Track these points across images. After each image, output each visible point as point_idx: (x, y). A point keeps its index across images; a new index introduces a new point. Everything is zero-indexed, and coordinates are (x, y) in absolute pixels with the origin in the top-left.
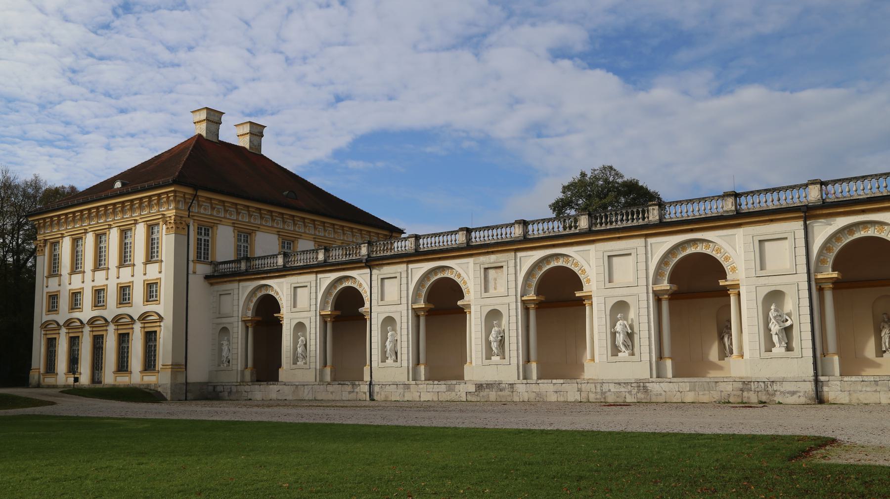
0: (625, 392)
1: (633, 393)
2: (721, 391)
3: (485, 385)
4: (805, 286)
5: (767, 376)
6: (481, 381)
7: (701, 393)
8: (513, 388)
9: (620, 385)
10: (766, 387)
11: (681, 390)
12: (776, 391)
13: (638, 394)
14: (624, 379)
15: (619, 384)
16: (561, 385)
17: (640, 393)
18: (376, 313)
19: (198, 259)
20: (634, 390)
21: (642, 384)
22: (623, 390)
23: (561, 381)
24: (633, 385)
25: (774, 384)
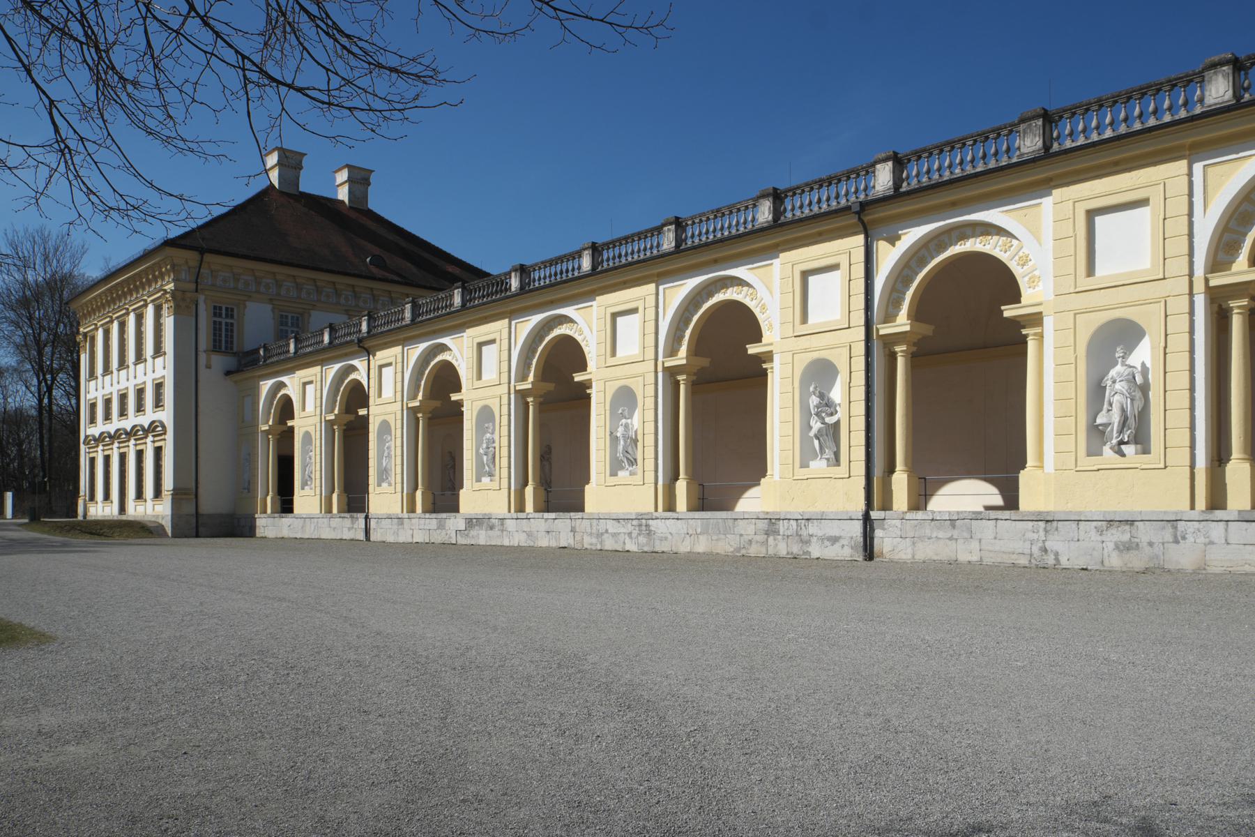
0: (625, 533)
2: (741, 535)
4: (860, 349)
5: (801, 510)
7: (715, 537)
8: (502, 524)
9: (619, 522)
10: (799, 528)
11: (690, 532)
12: (812, 536)
15: (618, 520)
18: (470, 402)
19: (216, 348)
20: (634, 531)
23: (553, 515)
24: (635, 522)
25: (810, 525)
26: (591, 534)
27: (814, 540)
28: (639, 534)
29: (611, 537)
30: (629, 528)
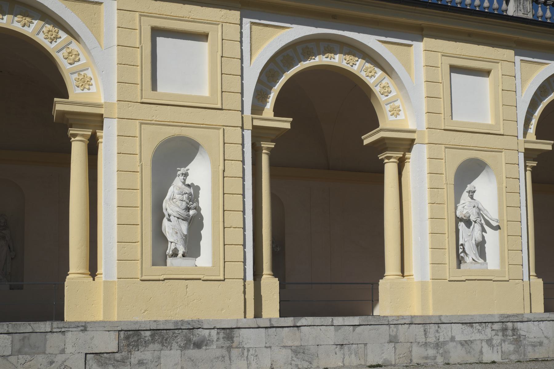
1: (494, 342)
3: (148, 333)
6: (137, 322)
9: (472, 327)
13: (503, 344)
14: (480, 316)
16: (354, 330)
17: (506, 343)
20: (496, 337)
22: (477, 336)
24: (496, 326)
26: (426, 344)
29: (459, 346)
30: (488, 332)
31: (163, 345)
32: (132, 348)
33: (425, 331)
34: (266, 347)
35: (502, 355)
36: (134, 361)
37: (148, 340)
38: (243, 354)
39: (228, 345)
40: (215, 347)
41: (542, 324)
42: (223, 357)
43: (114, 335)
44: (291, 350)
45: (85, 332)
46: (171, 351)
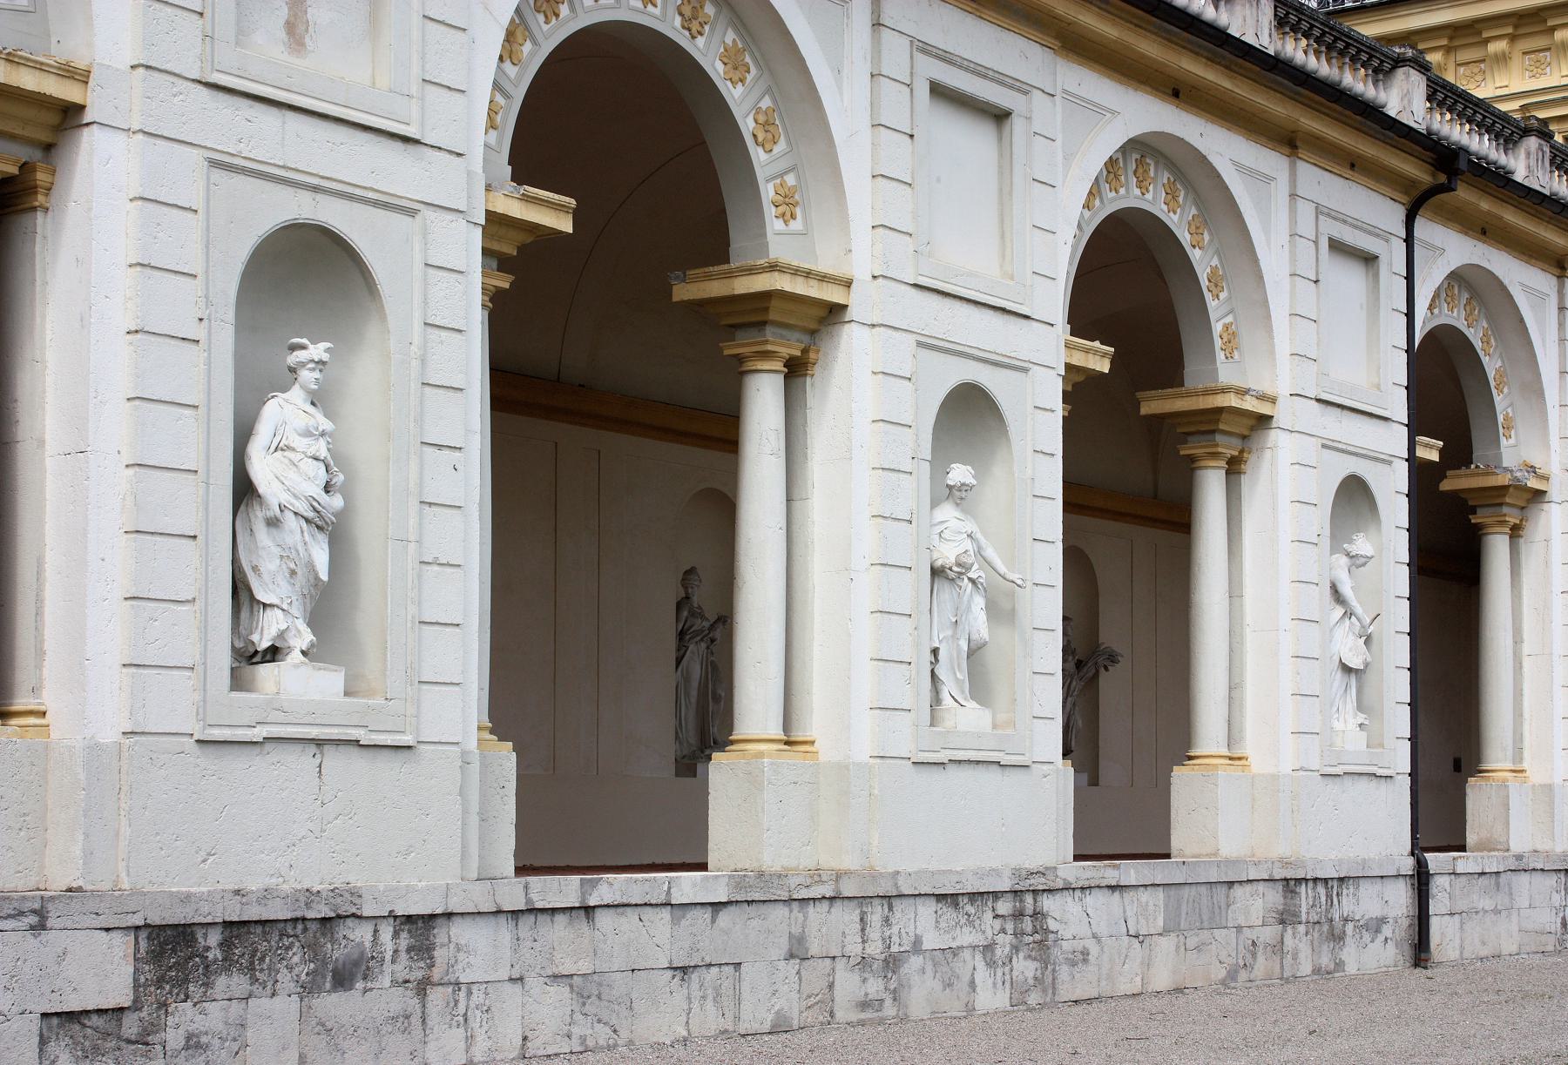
0: (974, 947)
2: (1239, 928)
6: (186, 898)
8: (423, 950)
12: (1346, 920)
15: (948, 899)
20: (1000, 938)
21: (1029, 899)
24: (1004, 907)
27: (1350, 927)
28: (1016, 949)
31: (254, 980)
32: (170, 992)
33: (862, 920)
34: (511, 979)
35: (1011, 993)
36: (174, 1038)
37: (216, 960)
38: (456, 1002)
39: (419, 974)
40: (387, 983)
41: (1094, 900)
42: (407, 1017)
43: (122, 945)
44: (571, 986)
45: (40, 934)
46: (275, 998)
